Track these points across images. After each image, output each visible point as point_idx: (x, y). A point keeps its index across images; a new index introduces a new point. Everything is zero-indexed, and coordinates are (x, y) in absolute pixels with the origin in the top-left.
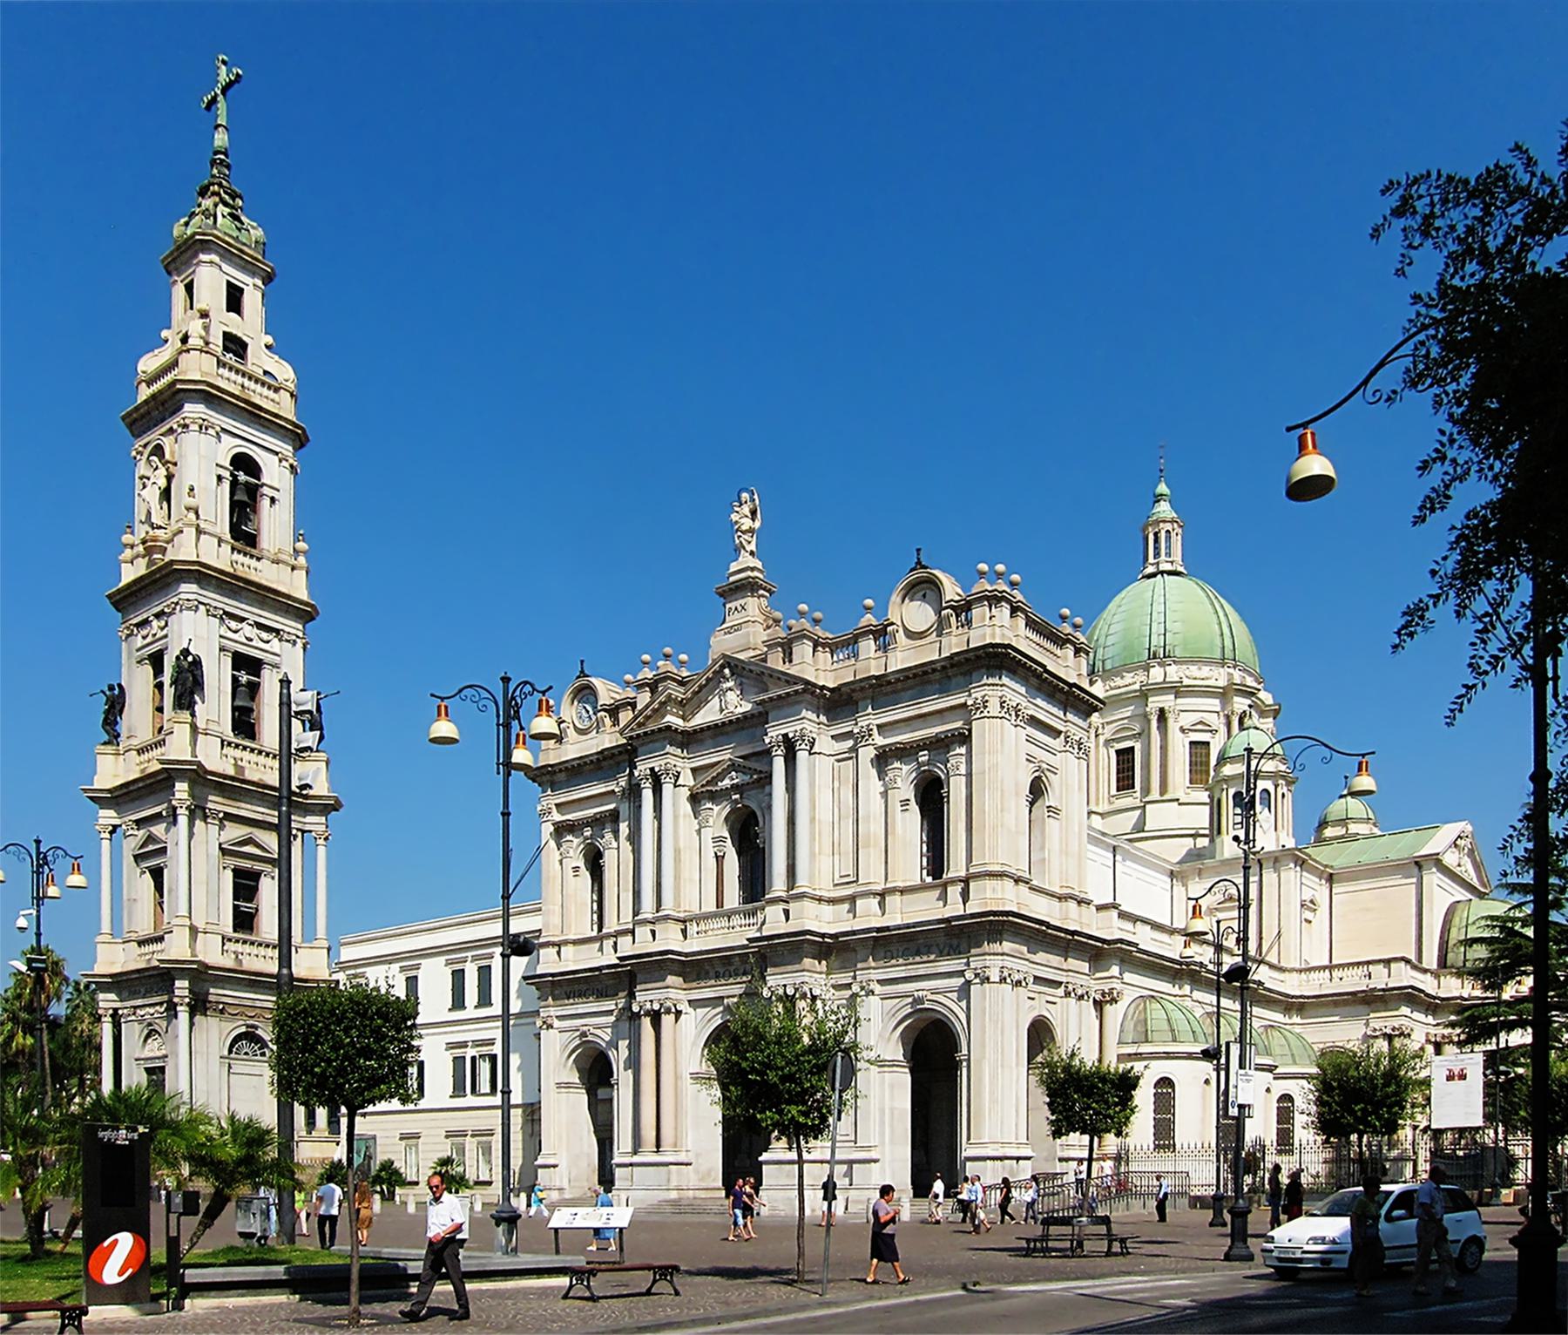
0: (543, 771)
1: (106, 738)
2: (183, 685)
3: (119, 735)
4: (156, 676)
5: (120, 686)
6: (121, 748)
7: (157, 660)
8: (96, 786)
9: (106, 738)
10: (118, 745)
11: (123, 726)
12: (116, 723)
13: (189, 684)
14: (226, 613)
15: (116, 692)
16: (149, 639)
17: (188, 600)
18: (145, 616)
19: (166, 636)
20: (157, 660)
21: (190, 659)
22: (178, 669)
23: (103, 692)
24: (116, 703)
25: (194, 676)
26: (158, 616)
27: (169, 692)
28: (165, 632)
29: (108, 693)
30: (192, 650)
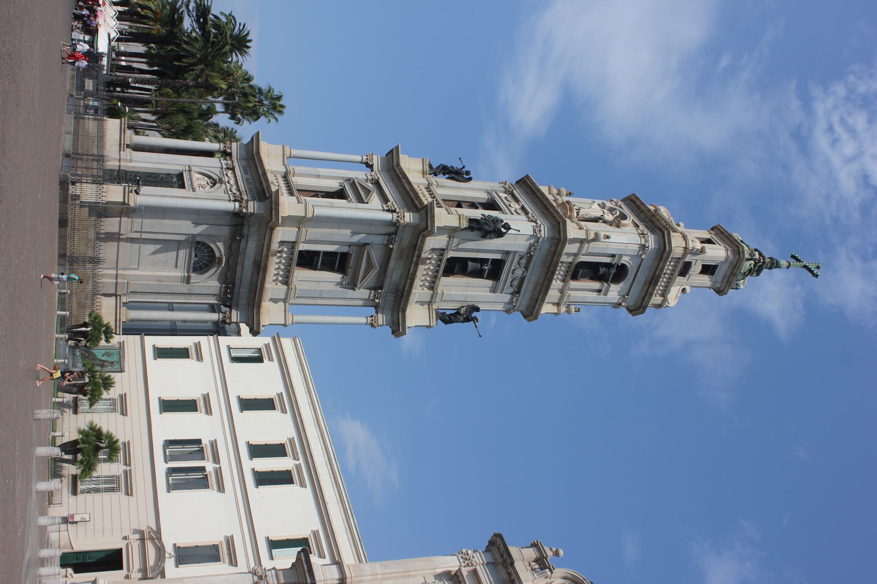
0: (505, 554)
1: (435, 166)
2: (486, 224)
3: (436, 175)
4: (481, 204)
5: (470, 179)
6: (428, 176)
7: (491, 205)
8: (401, 156)
9: (435, 166)
10: (430, 174)
11: (442, 179)
12: (444, 175)
13: (486, 227)
14: (531, 256)
15: (465, 176)
16: (505, 201)
17: (540, 231)
18: (521, 199)
19: (512, 214)
20: (491, 205)
21: (503, 230)
22: (496, 221)
23: (464, 167)
24: (457, 175)
25: (491, 232)
26: (523, 208)
27: (478, 214)
28: (515, 213)
29: (464, 170)
30: (510, 231)
